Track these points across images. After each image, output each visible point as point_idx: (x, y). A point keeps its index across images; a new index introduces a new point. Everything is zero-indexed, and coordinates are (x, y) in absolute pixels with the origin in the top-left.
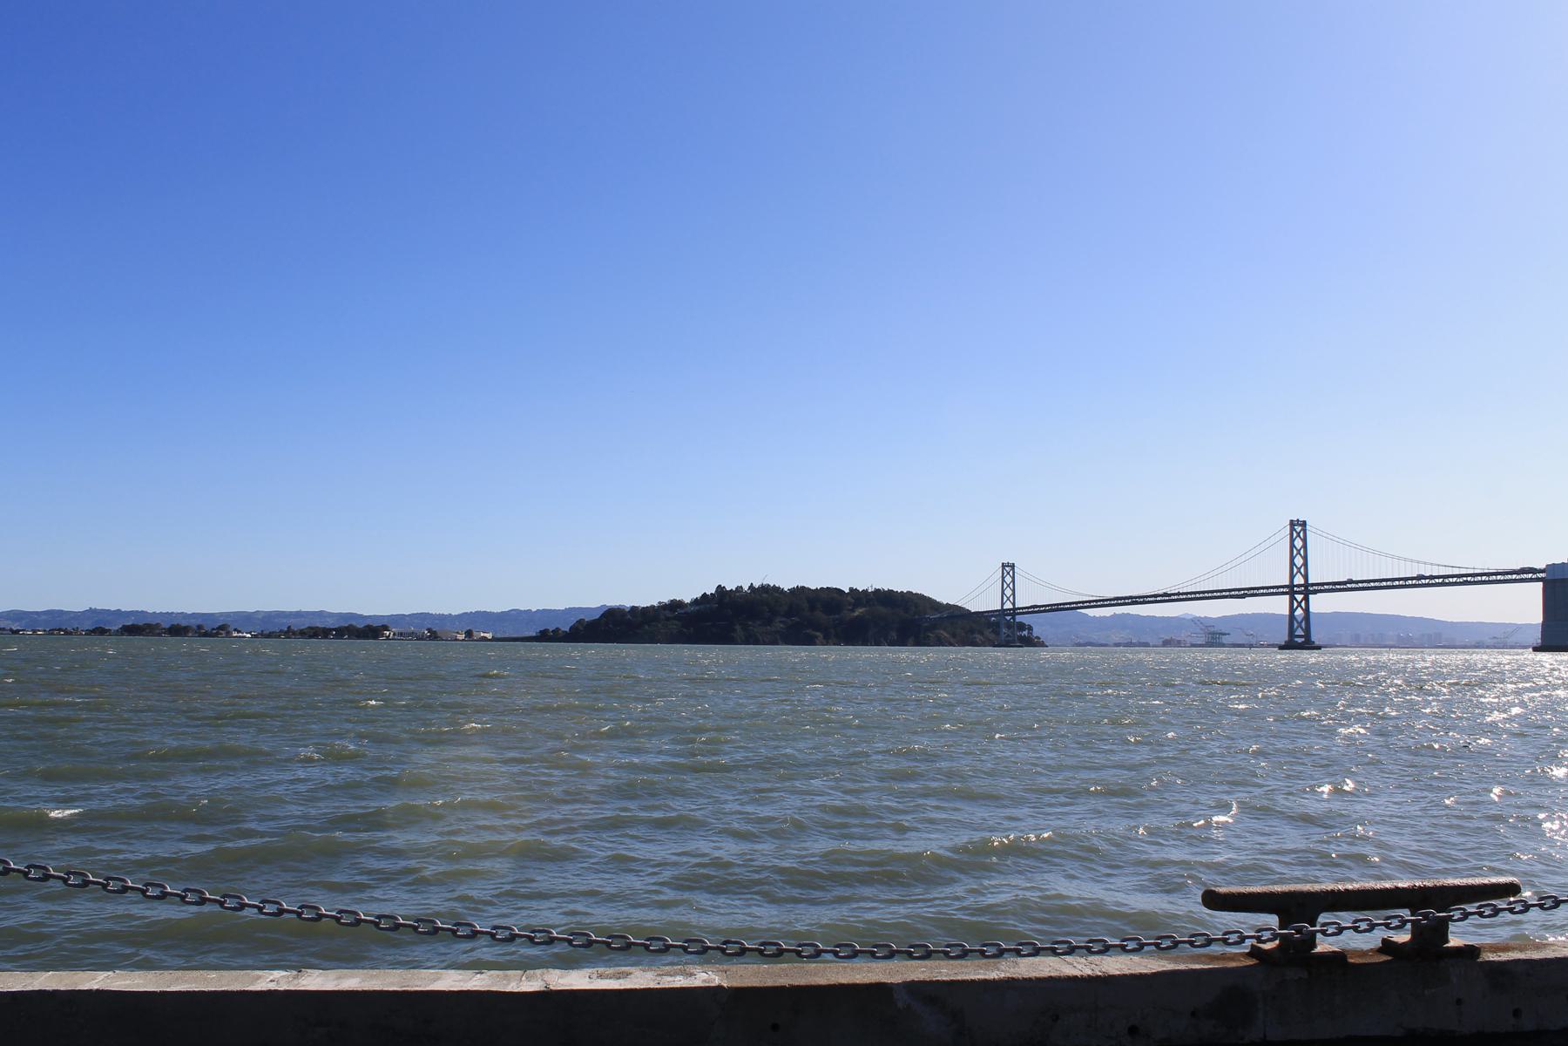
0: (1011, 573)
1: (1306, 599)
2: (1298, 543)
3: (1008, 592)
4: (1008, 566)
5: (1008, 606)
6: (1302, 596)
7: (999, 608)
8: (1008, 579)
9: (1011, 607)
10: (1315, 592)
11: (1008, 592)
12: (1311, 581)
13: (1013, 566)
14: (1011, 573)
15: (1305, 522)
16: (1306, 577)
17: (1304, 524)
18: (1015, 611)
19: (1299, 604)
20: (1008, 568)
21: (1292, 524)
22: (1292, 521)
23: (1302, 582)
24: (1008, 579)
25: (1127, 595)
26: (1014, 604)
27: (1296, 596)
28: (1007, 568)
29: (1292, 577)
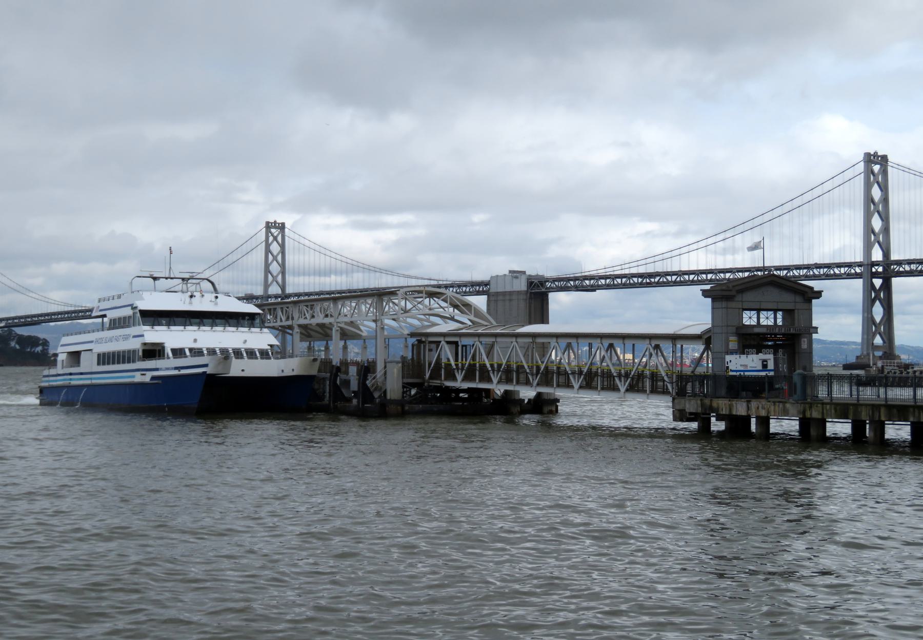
25: (40, 312)
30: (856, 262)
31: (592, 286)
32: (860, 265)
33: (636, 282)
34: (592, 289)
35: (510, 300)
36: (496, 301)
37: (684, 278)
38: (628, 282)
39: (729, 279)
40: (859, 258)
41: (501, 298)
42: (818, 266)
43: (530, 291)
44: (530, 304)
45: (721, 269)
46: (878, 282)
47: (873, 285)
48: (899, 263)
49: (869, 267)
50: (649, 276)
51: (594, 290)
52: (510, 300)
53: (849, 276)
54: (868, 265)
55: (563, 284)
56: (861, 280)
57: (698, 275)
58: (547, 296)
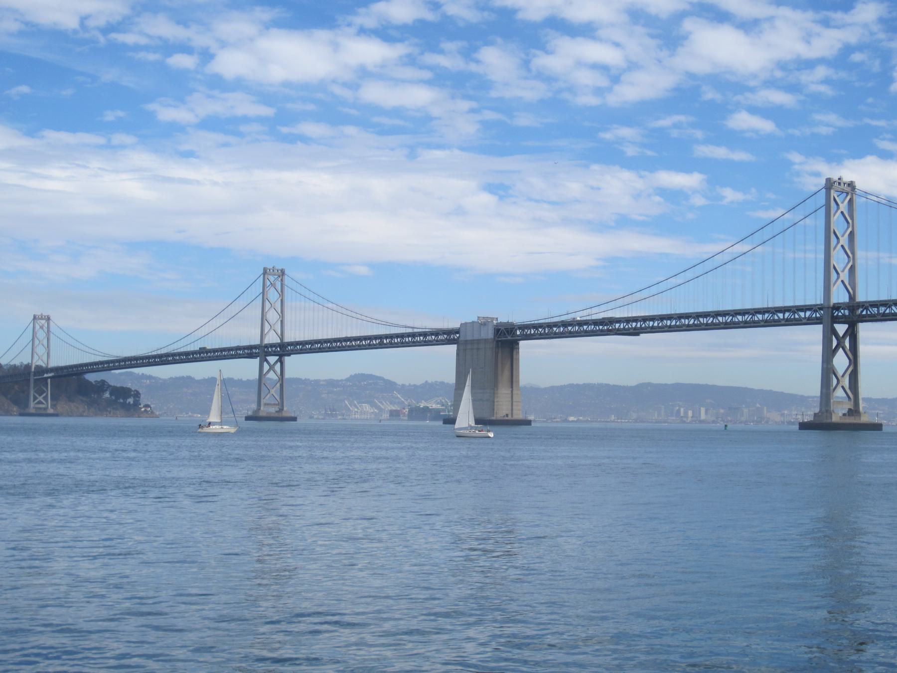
1: (852, 334)
3: (273, 316)
5: (272, 338)
6: (845, 327)
7: (259, 343)
8: (273, 295)
9: (277, 340)
10: (873, 319)
11: (273, 316)
12: (861, 298)
18: (284, 350)
19: (840, 344)
24: (273, 295)
26: (282, 339)
27: (837, 326)
28: (272, 278)
30: (817, 305)
31: (635, 328)
32: (820, 308)
33: (803, 316)
34: (636, 332)
35: (478, 349)
36: (465, 350)
37: (799, 315)
38: (793, 317)
39: (555, 332)
40: (819, 300)
41: (469, 347)
42: (783, 310)
43: (496, 339)
44: (497, 354)
45: (758, 309)
46: (841, 329)
47: (835, 332)
48: (865, 305)
49: (830, 310)
50: (610, 322)
51: (637, 334)
52: (478, 349)
53: (810, 321)
54: (828, 308)
55: (748, 318)
56: (820, 327)
57: (890, 307)
58: (518, 344)
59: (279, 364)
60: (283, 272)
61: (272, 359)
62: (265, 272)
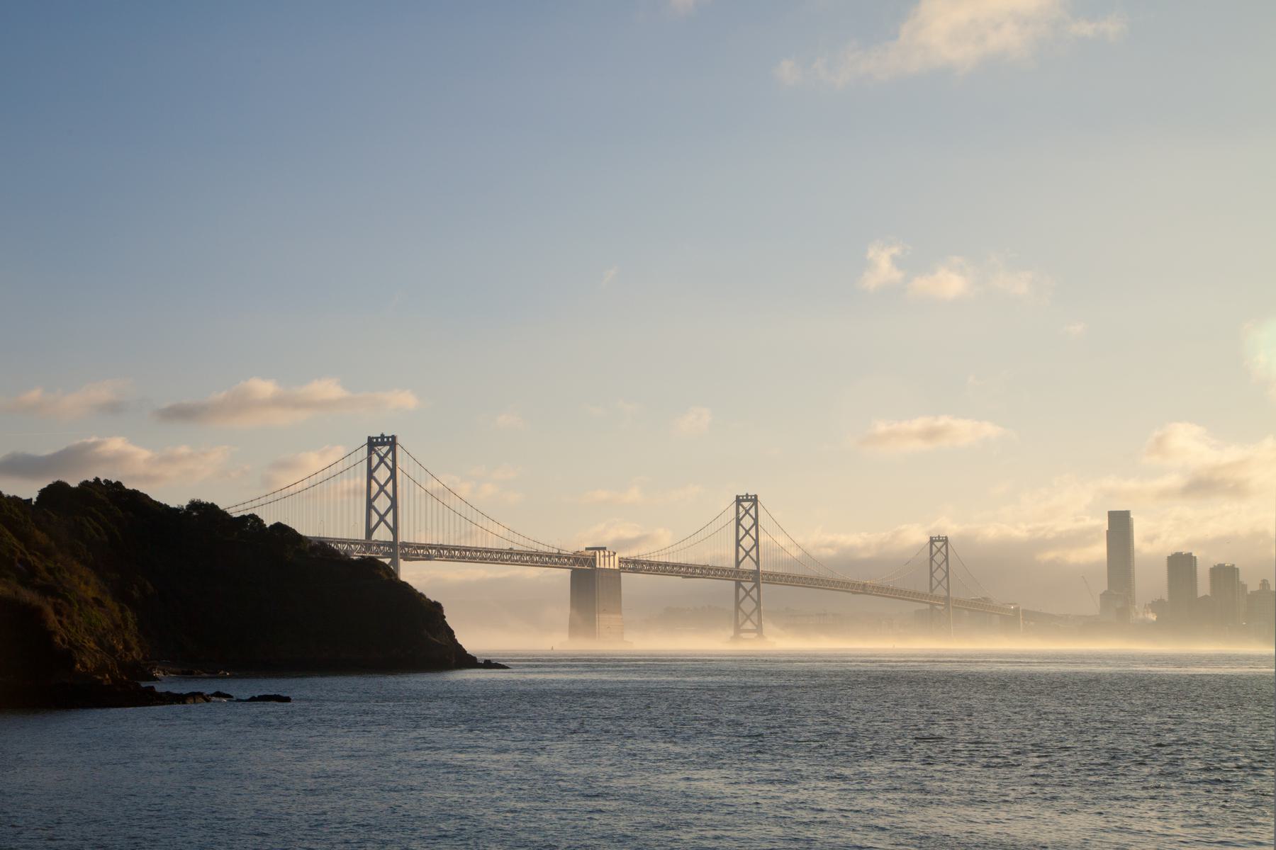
0: (752, 512)
2: (382, 474)
4: (747, 500)
5: (748, 565)
13: (755, 500)
14: (752, 512)
15: (394, 437)
16: (394, 530)
17: (392, 442)
20: (748, 503)
21: (372, 444)
22: (370, 439)
23: (390, 538)
24: (747, 522)
28: (743, 503)
29: (369, 532)
59: (755, 589)
60: (756, 496)
61: (748, 585)
62: (739, 501)
